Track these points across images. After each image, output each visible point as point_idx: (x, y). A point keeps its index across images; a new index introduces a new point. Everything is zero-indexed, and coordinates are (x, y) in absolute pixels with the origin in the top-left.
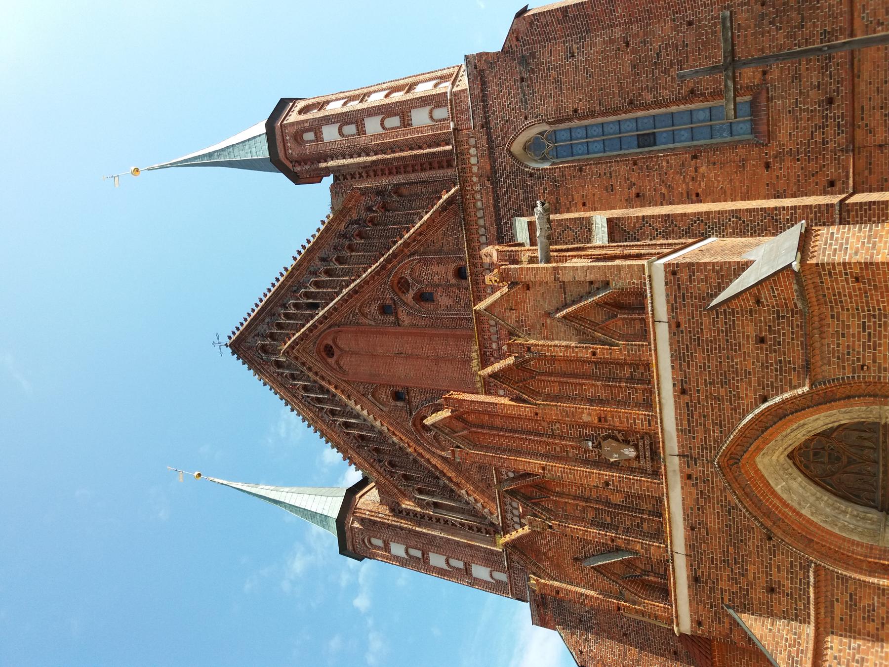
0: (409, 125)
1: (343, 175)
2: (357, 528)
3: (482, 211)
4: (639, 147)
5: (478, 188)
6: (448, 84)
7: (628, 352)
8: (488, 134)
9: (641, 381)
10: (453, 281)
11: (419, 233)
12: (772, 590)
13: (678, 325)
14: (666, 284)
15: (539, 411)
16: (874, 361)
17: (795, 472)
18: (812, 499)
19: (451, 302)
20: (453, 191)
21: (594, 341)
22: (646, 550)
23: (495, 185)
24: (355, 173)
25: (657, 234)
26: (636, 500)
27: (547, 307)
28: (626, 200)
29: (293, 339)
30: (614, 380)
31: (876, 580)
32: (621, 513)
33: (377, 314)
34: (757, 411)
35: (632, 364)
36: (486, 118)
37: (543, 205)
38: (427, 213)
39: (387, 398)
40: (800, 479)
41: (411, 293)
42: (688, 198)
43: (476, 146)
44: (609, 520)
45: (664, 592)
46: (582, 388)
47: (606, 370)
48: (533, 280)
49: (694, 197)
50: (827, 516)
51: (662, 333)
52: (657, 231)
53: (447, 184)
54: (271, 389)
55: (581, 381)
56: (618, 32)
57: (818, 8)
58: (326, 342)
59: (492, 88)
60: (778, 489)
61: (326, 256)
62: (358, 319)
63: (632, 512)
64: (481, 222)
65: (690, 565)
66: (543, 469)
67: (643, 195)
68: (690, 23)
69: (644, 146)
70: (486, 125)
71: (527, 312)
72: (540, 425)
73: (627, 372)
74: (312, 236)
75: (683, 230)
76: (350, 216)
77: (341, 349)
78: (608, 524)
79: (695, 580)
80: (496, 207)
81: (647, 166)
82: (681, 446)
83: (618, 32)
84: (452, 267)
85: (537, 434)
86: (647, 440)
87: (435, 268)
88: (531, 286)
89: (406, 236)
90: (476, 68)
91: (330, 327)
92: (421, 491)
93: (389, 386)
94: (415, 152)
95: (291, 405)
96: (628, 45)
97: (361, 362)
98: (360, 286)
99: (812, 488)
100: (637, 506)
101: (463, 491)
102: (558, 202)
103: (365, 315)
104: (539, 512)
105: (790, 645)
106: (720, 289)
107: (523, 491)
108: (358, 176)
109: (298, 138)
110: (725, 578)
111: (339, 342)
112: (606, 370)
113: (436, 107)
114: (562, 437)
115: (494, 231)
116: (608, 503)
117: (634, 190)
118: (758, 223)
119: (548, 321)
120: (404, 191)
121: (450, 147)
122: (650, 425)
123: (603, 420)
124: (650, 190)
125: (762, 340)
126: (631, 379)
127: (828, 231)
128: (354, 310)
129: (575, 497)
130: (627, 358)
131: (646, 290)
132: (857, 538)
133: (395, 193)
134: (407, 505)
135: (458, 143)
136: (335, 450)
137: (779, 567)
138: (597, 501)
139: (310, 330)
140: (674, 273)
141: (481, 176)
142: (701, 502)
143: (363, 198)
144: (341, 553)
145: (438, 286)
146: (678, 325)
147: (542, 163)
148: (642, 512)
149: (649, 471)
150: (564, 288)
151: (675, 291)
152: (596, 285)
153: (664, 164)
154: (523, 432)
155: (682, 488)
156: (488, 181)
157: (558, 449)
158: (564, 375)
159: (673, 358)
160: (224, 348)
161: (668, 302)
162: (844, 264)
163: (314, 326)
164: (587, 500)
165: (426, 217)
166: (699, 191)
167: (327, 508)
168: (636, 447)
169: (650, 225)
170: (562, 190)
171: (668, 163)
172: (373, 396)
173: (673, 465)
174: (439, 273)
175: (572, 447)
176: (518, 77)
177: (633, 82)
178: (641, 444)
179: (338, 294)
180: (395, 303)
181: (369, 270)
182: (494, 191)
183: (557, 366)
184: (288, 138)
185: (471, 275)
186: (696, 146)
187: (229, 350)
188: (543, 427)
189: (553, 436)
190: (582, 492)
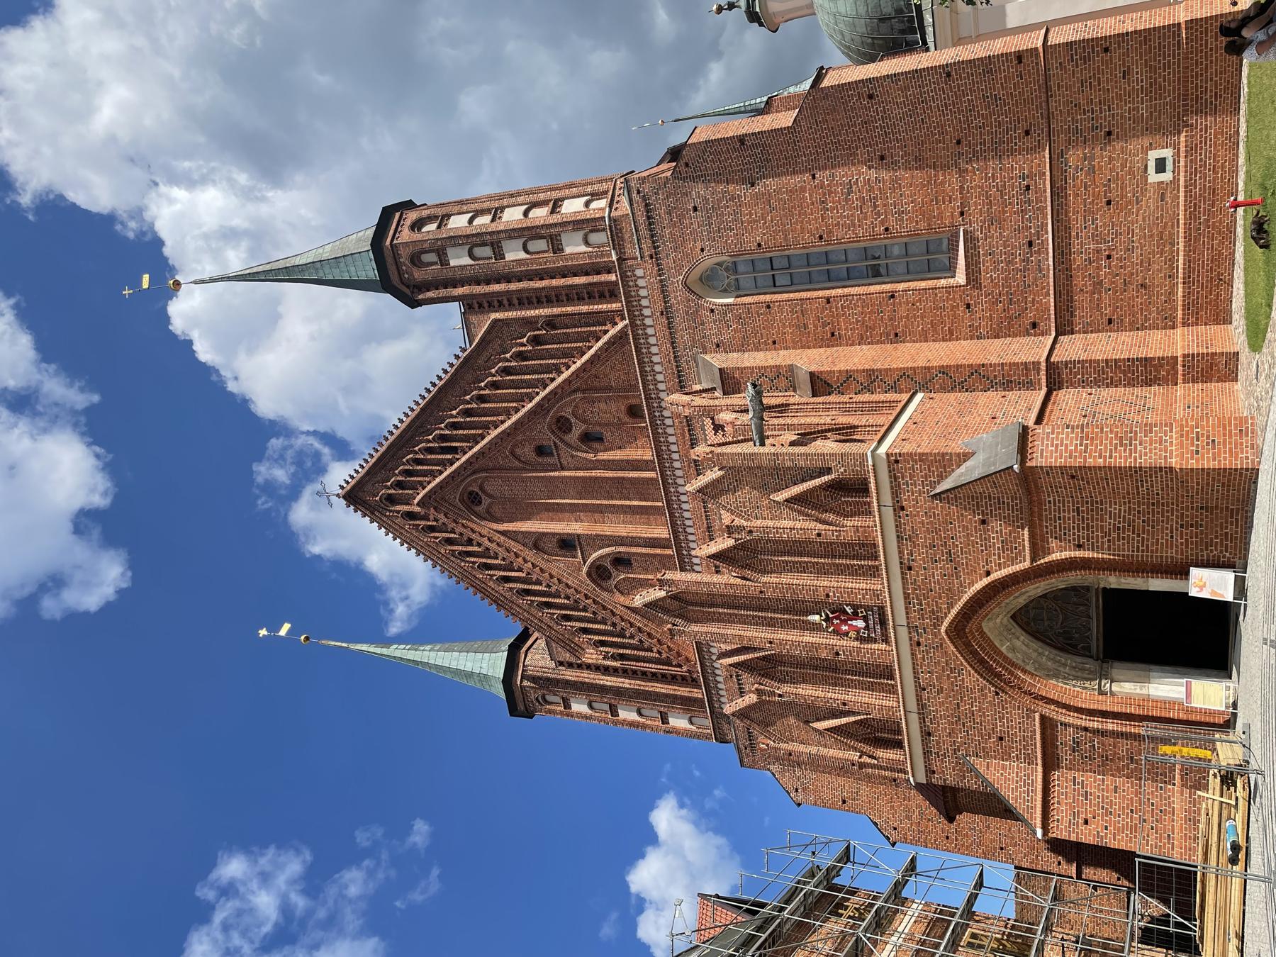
0: (559, 250)
2: (528, 687)
6: (602, 203)
10: (627, 419)
17: (1018, 631)
18: (1034, 655)
20: (621, 325)
36: (655, 248)
37: (754, 388)
40: (1024, 637)
53: (610, 318)
58: (471, 489)
60: (1003, 649)
66: (771, 643)
77: (490, 496)
87: (603, 406)
90: (639, 192)
99: (1035, 645)
105: (1021, 785)
109: (416, 260)
111: (488, 488)
113: (592, 231)
118: (966, 379)
121: (613, 277)
127: (1044, 430)
128: (504, 453)
160: (334, 499)
167: (484, 665)
168: (865, 619)
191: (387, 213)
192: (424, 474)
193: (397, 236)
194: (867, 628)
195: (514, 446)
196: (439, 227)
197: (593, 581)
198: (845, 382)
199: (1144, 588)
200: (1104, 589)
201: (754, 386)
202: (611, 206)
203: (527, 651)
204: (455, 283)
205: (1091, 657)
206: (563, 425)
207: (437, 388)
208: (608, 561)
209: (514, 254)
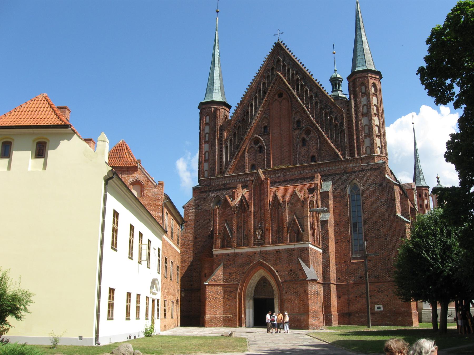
1: (349, 105)
3: (334, 168)
4: (353, 223)
5: (342, 167)
8: (360, 171)
9: (279, 240)
10: (310, 155)
11: (327, 141)
12: (230, 274)
13: (294, 250)
14: (304, 247)
16: (288, 295)
17: (260, 277)
18: (254, 282)
19: (303, 154)
20: (341, 157)
21: (289, 227)
23: (343, 174)
24: (349, 111)
27: (297, 213)
29: (284, 78)
30: (278, 233)
31: (238, 297)
34: (274, 270)
36: (365, 170)
38: (334, 145)
39: (264, 123)
40: (259, 279)
41: (305, 136)
43: (356, 166)
44: (239, 230)
45: (223, 247)
48: (304, 209)
49: (337, 241)
50: (251, 285)
51: (292, 246)
54: (262, 65)
56: (386, 217)
57: (385, 274)
58: (284, 94)
59: (374, 172)
60: (255, 274)
61: (318, 95)
64: (331, 168)
65: (232, 253)
66: (251, 212)
68: (386, 239)
69: (353, 225)
70: (363, 170)
73: (281, 236)
76: (334, 108)
79: (228, 255)
80: (336, 174)
82: (263, 251)
83: (386, 217)
87: (315, 147)
89: (326, 136)
90: (381, 166)
91: (290, 96)
92: (231, 140)
93: (269, 125)
94: (355, 140)
95: (257, 76)
96: (382, 220)
98: (307, 114)
99: (257, 282)
101: (234, 160)
103: (296, 113)
106: (303, 261)
108: (348, 112)
109: (363, 84)
110: (230, 262)
114: (260, 217)
115: (328, 173)
116: (244, 230)
119: (293, 213)
120: (342, 134)
121: (356, 155)
125: (291, 271)
126: (279, 237)
129: (244, 221)
132: (246, 292)
133: (341, 130)
134: (225, 134)
135: (357, 159)
136: (241, 99)
137: (236, 275)
138: (244, 227)
139: (288, 88)
140: (307, 249)
142: (249, 256)
144: (200, 103)
145: (308, 148)
146: (294, 250)
148: (244, 240)
153: (347, 232)
154: (260, 205)
155: (252, 252)
156: (345, 171)
157: (257, 215)
159: (285, 249)
160: (276, 38)
161: (299, 248)
162: (308, 289)
163: (290, 90)
164: (244, 224)
165: (332, 145)
172: (265, 117)
173: (258, 249)
174: (313, 149)
175: (258, 220)
176: (376, 182)
177: (371, 222)
179: (303, 103)
181: (313, 119)
182: (342, 173)
184: (363, 79)
185: (312, 164)
187: (276, 42)
189: (260, 214)
191: (378, 73)
192: (289, 76)
193: (371, 78)
194: (258, 239)
196: (373, 94)
199: (275, 307)
200: (274, 298)
202: (378, 156)
203: (223, 108)
204: (355, 98)
205: (254, 296)
207: (319, 86)
208: (261, 144)
209: (364, 121)
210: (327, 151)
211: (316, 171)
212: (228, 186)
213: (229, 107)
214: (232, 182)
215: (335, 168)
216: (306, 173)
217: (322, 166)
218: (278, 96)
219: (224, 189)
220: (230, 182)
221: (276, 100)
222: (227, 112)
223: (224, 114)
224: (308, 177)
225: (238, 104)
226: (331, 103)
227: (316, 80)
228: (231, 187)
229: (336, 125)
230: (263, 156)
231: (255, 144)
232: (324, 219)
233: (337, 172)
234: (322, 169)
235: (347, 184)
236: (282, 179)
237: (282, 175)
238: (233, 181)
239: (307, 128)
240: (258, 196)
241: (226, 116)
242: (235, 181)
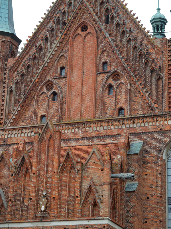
3: (147, 125)
4: (168, 198)
5: (158, 124)
7: (78, 210)
9: (68, 213)
10: (118, 107)
14: (101, 224)
15: (55, 173)
22: (8, 213)
25: (128, 210)
26: (26, 209)
27: (94, 178)
28: (146, 193)
30: (68, 204)
32: (20, 203)
33: (103, 60)
35: (74, 211)
39: (61, 64)
42: (145, 219)
44: (18, 198)
46: (65, 191)
47: (72, 200)
49: (146, 221)
52: (129, 210)
55: (67, 191)
58: (89, 27)
62: (100, 49)
63: (22, 208)
64: (143, 125)
66: (34, 174)
67: (148, 200)
69: (168, 200)
71: (93, 170)
72: (51, 173)
73: (71, 208)
74: (142, 24)
75: (129, 220)
77: (85, 37)
78: (16, 198)
81: (159, 202)
82: (47, 227)
84: (124, 106)
85: (47, 171)
86: (47, 215)
87: (124, 97)
88: (102, 171)
97: (79, 49)
100: (24, 209)
102: (148, 163)
104: (17, 170)
107: (25, 163)
111: (89, 35)
112: (72, 200)
115: (138, 131)
116: (24, 198)
117: (150, 196)
119: (89, 178)
120: (160, 82)
122: (53, 216)
123: (54, 199)
124: (150, 203)
126: (69, 210)
128: (105, 47)
129: (24, 185)
130: (76, 209)
131: (99, 217)
133: (159, 77)
136: (34, 31)
138: (24, 194)
141: (162, 126)
143: (159, 57)
147: (166, 155)
148: (22, 212)
149: (37, 215)
150: (101, 185)
151: (98, 227)
152: (102, 198)
153: (159, 209)
154: (47, 165)
155: (32, 227)
156: (161, 129)
157: (42, 179)
158: (70, 184)
161: (95, 225)
164: (24, 190)
166: (148, 223)
168: (45, 211)
169: (131, 208)
170: (153, 165)
171: (159, 211)
172: (62, 55)
173: (40, 225)
175: (43, 185)
178: (46, 213)
180: (108, 72)
183: (73, 181)
186: (166, 221)
188: (50, 174)
189: (47, 178)
190: (27, 188)
194: (41, 211)
195: (107, 51)
197: (46, 82)
198: (131, 204)
201: (133, 176)
206: (116, 76)
210: (139, 103)
211: (124, 127)
212: (9, 142)
213: (19, 41)
214: (14, 136)
215: (148, 124)
216: (111, 129)
217: (131, 122)
218: (81, 29)
219: (3, 145)
220: (13, 136)
221: (78, 34)
222: (15, 47)
223: (11, 50)
224: (112, 135)
225: (29, 37)
226: (149, 42)
227: (131, 11)
228: (13, 142)
229: (153, 71)
230: (56, 105)
231: (47, 89)
232: (131, 190)
233: (151, 131)
234: (131, 126)
235: (162, 146)
236: (79, 136)
237: (80, 131)
238: (16, 135)
239: (116, 71)
240: (45, 154)
241: (13, 51)
242: (19, 135)
